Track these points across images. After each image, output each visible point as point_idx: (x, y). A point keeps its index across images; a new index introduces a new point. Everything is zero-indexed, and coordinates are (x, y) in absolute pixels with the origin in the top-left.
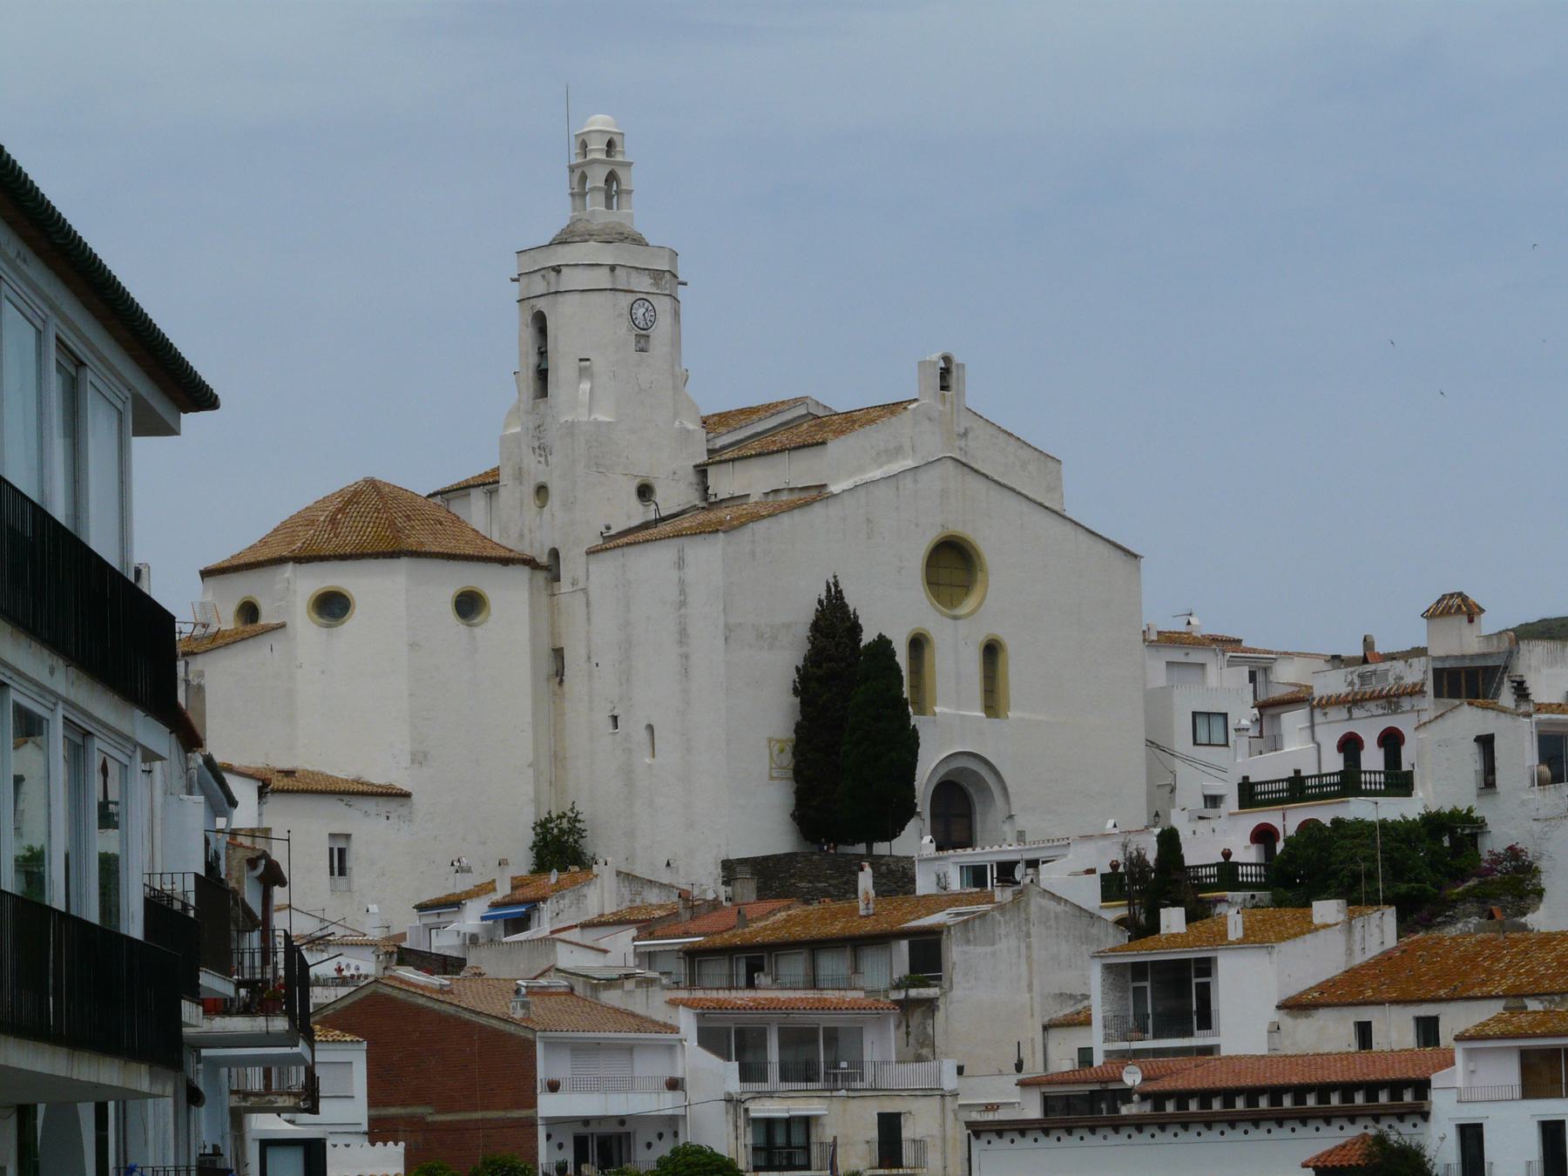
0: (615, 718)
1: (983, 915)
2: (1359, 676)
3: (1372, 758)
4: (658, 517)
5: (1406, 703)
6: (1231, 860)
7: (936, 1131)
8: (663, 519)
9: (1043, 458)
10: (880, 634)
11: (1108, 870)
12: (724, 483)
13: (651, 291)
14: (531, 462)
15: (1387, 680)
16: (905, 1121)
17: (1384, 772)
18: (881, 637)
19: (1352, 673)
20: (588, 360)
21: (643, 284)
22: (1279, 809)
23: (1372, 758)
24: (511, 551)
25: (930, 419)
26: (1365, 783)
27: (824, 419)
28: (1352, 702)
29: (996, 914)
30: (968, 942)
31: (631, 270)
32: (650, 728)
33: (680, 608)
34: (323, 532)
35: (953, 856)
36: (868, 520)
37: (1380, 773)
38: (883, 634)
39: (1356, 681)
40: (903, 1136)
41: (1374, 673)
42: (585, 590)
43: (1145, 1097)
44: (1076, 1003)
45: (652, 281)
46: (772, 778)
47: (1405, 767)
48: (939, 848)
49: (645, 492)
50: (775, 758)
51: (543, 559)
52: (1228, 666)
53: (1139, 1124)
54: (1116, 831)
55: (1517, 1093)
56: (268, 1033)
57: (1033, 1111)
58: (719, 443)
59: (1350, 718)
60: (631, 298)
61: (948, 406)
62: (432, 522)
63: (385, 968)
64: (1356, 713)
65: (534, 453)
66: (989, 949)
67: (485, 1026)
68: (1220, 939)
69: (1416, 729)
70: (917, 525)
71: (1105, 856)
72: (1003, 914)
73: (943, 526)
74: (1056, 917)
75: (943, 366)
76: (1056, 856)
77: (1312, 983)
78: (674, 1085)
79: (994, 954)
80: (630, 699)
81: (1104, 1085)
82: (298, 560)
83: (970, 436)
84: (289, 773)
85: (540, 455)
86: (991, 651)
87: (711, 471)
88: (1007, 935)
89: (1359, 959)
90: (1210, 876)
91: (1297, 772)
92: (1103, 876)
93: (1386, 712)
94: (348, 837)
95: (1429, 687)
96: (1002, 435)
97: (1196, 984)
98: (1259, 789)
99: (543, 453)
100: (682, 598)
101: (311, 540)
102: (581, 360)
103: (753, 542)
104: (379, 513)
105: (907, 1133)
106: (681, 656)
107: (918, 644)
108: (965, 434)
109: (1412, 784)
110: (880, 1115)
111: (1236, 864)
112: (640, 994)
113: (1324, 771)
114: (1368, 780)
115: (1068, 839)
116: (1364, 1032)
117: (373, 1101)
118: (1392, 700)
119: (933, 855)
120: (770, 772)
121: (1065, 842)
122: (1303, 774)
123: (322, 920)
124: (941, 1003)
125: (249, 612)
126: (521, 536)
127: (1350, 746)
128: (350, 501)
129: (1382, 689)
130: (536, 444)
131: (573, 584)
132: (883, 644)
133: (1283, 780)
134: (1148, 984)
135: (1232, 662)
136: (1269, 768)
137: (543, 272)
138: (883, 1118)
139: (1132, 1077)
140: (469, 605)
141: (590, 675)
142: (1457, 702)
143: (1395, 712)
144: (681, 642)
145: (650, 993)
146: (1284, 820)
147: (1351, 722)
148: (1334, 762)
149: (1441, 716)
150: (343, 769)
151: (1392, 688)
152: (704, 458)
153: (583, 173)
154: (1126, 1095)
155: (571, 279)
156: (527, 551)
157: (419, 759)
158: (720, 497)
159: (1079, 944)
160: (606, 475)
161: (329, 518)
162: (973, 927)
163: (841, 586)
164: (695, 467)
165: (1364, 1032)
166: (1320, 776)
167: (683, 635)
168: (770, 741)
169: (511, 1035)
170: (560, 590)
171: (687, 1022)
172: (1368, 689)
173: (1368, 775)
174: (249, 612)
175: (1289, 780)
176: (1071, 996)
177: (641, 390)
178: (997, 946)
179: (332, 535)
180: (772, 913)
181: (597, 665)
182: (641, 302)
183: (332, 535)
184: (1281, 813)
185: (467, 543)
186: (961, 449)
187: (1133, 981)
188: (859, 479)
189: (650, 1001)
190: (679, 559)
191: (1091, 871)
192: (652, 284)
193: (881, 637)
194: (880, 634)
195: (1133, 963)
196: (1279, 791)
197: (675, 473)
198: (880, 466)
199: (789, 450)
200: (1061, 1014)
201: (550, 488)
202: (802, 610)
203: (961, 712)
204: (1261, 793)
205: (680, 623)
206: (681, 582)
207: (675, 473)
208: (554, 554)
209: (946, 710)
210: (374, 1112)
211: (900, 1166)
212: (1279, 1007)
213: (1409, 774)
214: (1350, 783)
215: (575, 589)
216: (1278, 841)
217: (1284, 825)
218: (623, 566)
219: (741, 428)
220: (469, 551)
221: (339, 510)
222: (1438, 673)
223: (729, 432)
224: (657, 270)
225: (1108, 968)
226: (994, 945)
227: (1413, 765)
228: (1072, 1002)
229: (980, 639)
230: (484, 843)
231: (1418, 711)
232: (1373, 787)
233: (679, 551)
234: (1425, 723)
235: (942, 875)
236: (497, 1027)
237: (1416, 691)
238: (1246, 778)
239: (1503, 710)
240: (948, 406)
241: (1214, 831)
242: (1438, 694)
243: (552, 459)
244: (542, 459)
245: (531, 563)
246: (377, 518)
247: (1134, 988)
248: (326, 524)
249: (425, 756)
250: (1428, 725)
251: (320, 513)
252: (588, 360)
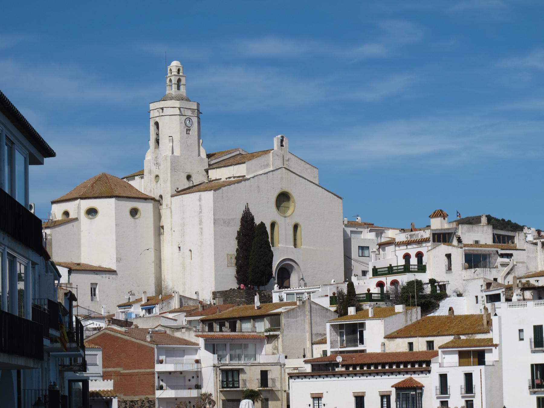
0: (180, 248)
1: (293, 309)
2: (410, 235)
3: (414, 261)
4: (193, 185)
5: (424, 245)
6: (370, 292)
7: (279, 376)
8: (195, 186)
9: (312, 167)
10: (262, 222)
11: (332, 295)
12: (214, 174)
13: (191, 115)
14: (154, 168)
15: (418, 237)
16: (269, 373)
17: (417, 265)
18: (262, 222)
19: (407, 234)
20: (172, 137)
21: (189, 113)
22: (385, 277)
23: (414, 261)
24: (147, 195)
25: (277, 155)
26: (412, 269)
27: (245, 155)
28: (407, 243)
29: (298, 309)
30: (288, 317)
31: (185, 109)
32: (190, 251)
33: (200, 214)
34: (89, 190)
35: (284, 291)
36: (258, 186)
37: (416, 265)
38: (263, 222)
39: (409, 237)
40: (268, 377)
41: (414, 234)
42: (170, 208)
43: (343, 366)
44: (322, 337)
45: (191, 112)
46: (228, 266)
47: (424, 264)
48: (280, 288)
49: (189, 177)
50: (229, 260)
51: (157, 198)
52: (369, 232)
53: (341, 375)
54: (335, 283)
55: (458, 365)
56: (70, 348)
57: (308, 368)
58: (212, 162)
59: (407, 249)
60: (185, 117)
61: (283, 151)
62: (123, 187)
63: (108, 325)
64: (409, 247)
65: (155, 166)
66: (295, 320)
67: (139, 343)
68: (366, 317)
69: (427, 252)
70: (273, 188)
71: (330, 291)
72: (299, 309)
73: (281, 188)
74: (316, 310)
75: (282, 139)
76: (316, 291)
77: (395, 330)
78: (197, 362)
79: (296, 321)
80: (184, 242)
81: (330, 362)
82: (82, 198)
83: (290, 160)
84: (79, 264)
85: (157, 166)
86: (296, 227)
87: (209, 171)
88: (301, 315)
89: (409, 323)
90: (364, 297)
91: (391, 265)
92: (330, 297)
93: (418, 246)
94: (96, 284)
95: (431, 239)
96: (300, 161)
97: (359, 331)
98: (379, 270)
99: (157, 165)
100: (200, 210)
101: (86, 192)
102: (169, 137)
103: (223, 193)
104: (106, 184)
105: (269, 377)
106: (200, 228)
107: (273, 225)
108: (288, 160)
109: (426, 269)
110: (261, 371)
111: (372, 294)
112: (187, 333)
113: (398, 265)
114: (412, 267)
115: (320, 285)
116: (411, 345)
117: (104, 366)
118: (420, 242)
119: (278, 290)
120: (228, 265)
121: (319, 286)
122: (392, 266)
123: (88, 310)
124: (280, 336)
125: (66, 213)
126: (151, 191)
127: (407, 257)
128: (97, 180)
129: (417, 240)
130: (155, 163)
131: (167, 206)
132: (262, 225)
133: (386, 268)
134: (344, 331)
135: (371, 231)
136: (382, 264)
137: (158, 109)
138: (262, 371)
139: (339, 359)
140: (134, 212)
141: (172, 234)
142: (440, 243)
143: (421, 247)
144: (200, 224)
145: (190, 333)
146: (386, 280)
147: (407, 250)
148: (402, 262)
149: (435, 248)
150: (95, 263)
151: (420, 239)
152: (207, 167)
153: (170, 79)
154: (337, 365)
155: (167, 111)
156: (152, 195)
157: (118, 260)
158: (212, 179)
159: (323, 318)
160: (177, 173)
161: (91, 185)
162: (290, 313)
163: (249, 207)
164: (204, 170)
165: (411, 345)
166: (398, 266)
167: (201, 222)
168: (228, 254)
169: (147, 346)
170: (162, 208)
171: (201, 342)
172: (413, 239)
173: (412, 266)
174: (66, 213)
175: (388, 267)
176: (320, 334)
177: (188, 146)
178: (298, 319)
179: (92, 191)
180: (228, 308)
181: (174, 231)
182: (188, 119)
183: (92, 191)
184: (385, 278)
185: (134, 193)
186: (287, 165)
187: (340, 329)
188: (255, 174)
189: (190, 335)
191: (327, 296)
192: (191, 113)
193: (262, 222)
194: (262, 222)
195: (339, 324)
196: (385, 271)
197: (198, 172)
198: (262, 170)
199: (234, 165)
200: (317, 340)
201: (160, 176)
202: (238, 215)
203: (287, 246)
204: (379, 272)
205: (200, 218)
206: (200, 205)
207: (198, 172)
208: (161, 197)
209: (282, 245)
210: (105, 370)
211: (268, 387)
212: (385, 338)
213: (425, 266)
214: (407, 269)
215: (167, 207)
216: (385, 286)
217: (386, 282)
218: (182, 200)
219: (219, 158)
220: (134, 196)
221: (94, 183)
222: (434, 235)
223: (215, 159)
224: (193, 109)
225: (332, 325)
226: (296, 318)
227: (426, 263)
228: (321, 336)
229: (293, 224)
230: (139, 286)
231: (428, 246)
232: (414, 270)
233: (199, 196)
234: (430, 250)
235: (281, 297)
236: (142, 343)
237: (427, 240)
238: (374, 267)
239: (454, 246)
240: (283, 151)
241: (365, 283)
242: (434, 241)
243: (161, 167)
244: (157, 167)
245: (153, 199)
246: (106, 185)
247: (340, 332)
248: (90, 187)
249: (121, 259)
250: (431, 251)
251: (88, 184)
252: (172, 137)
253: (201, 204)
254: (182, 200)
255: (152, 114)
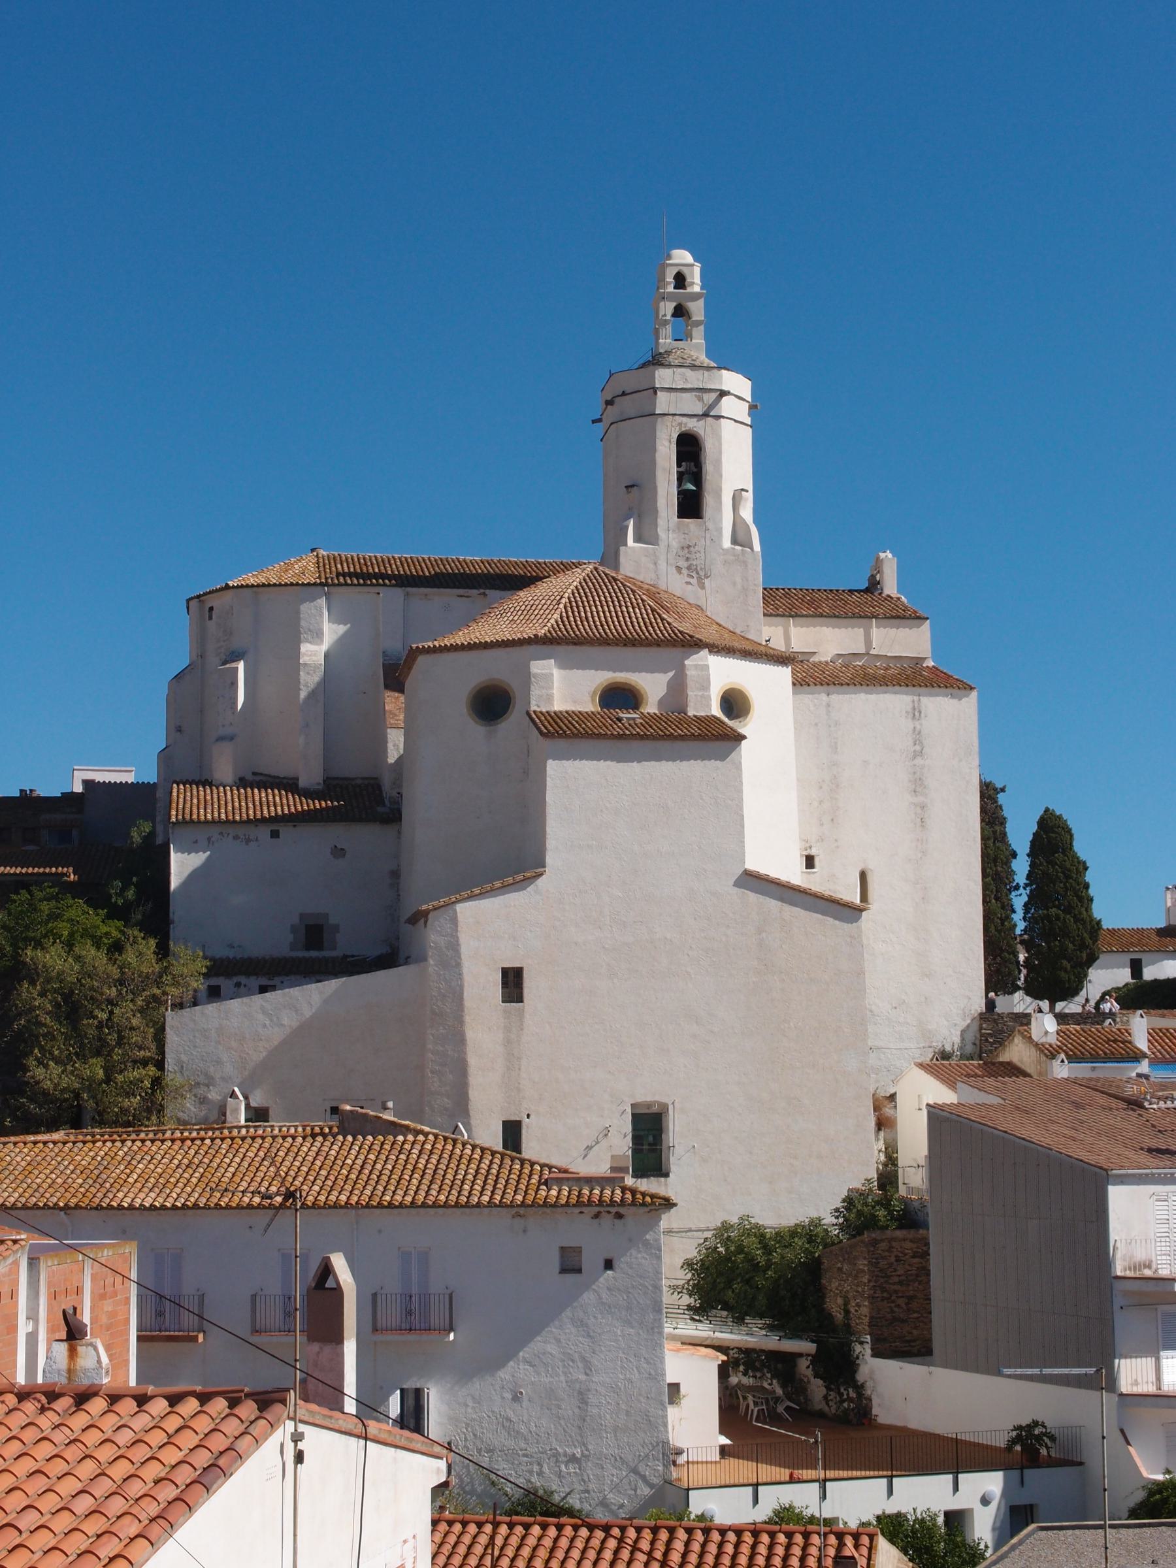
99: (694, 574)
100: (918, 748)
106: (916, 805)
144: (915, 792)
190: (914, 709)
205: (915, 773)
218: (828, 705)
244: (694, 581)
253: (918, 727)
254: (828, 705)
255: (663, 403)
